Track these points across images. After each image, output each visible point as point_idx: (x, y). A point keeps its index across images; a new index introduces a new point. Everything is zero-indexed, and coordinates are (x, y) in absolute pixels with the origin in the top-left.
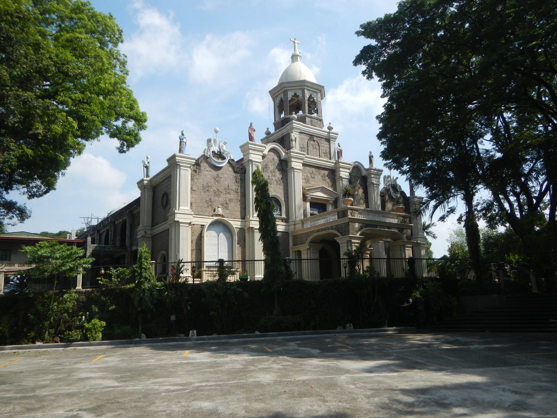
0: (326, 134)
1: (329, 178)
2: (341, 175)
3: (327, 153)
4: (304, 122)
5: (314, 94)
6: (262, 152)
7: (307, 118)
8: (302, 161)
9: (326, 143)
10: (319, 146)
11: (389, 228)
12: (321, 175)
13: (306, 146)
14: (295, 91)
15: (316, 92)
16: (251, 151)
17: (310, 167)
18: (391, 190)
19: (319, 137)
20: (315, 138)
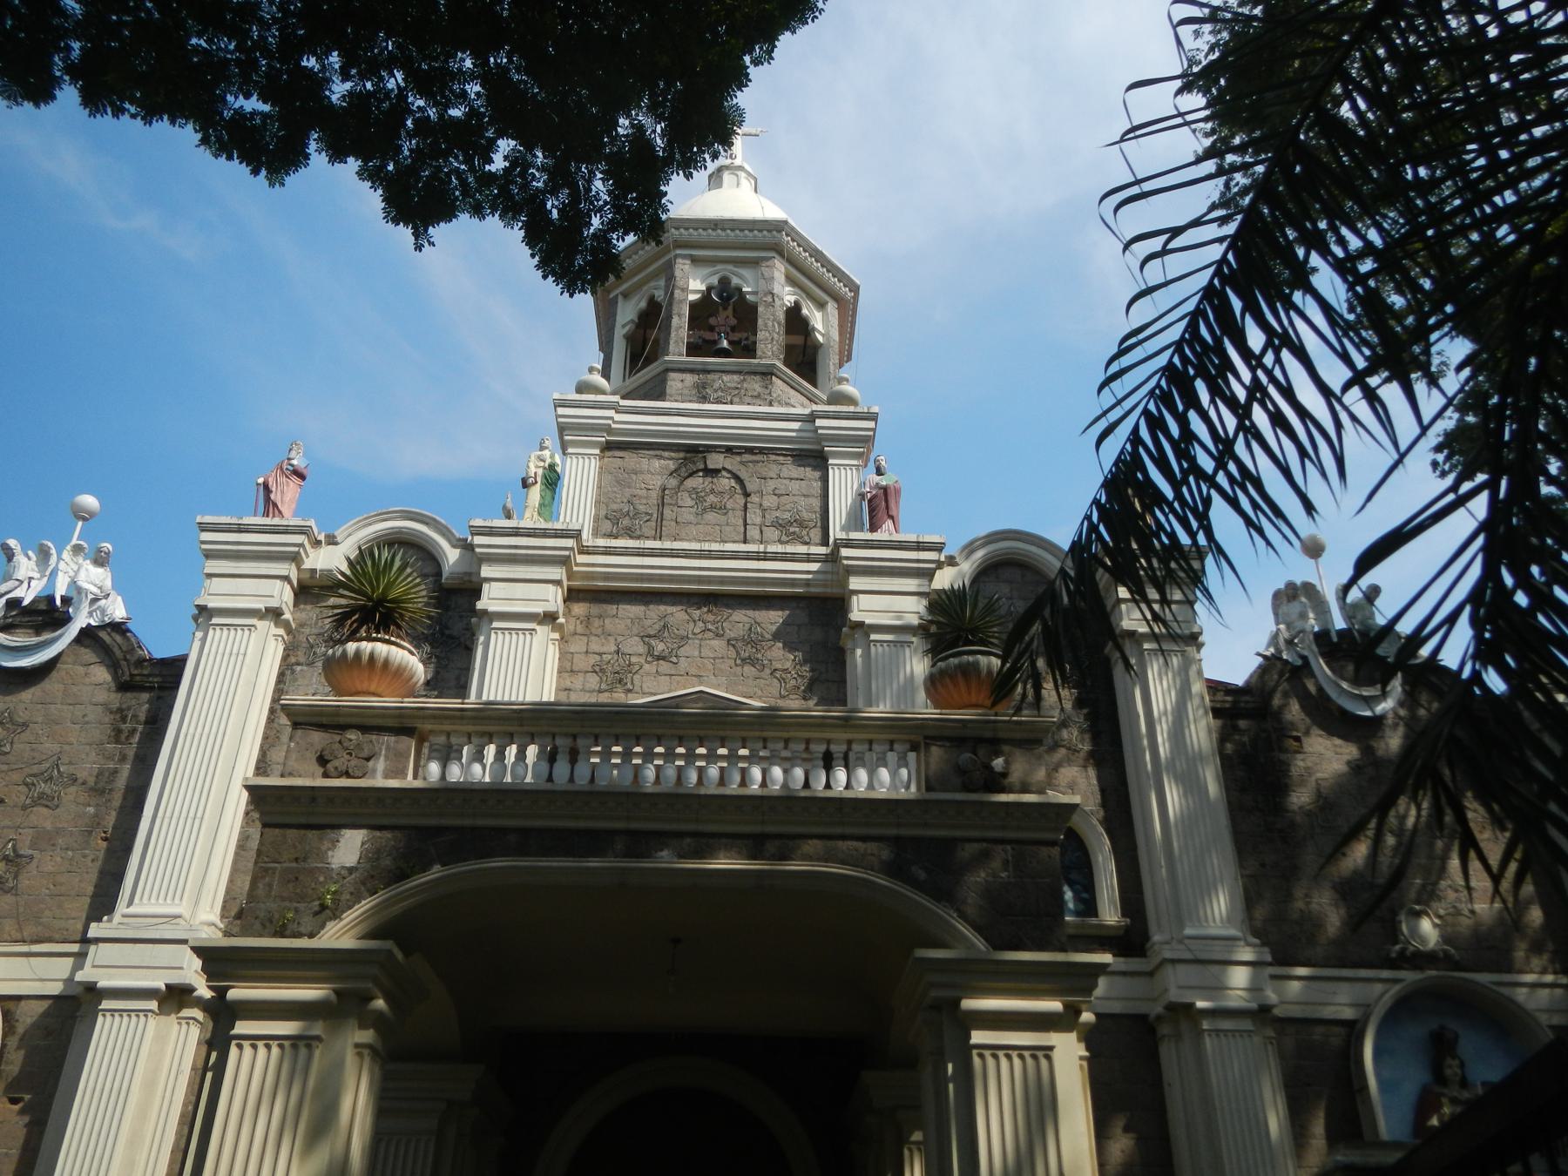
0: (796, 425)
1: (790, 647)
2: (855, 616)
3: (801, 524)
4: (661, 396)
5: (746, 273)
6: (295, 558)
7: (672, 375)
8: (557, 573)
9: (791, 470)
10: (747, 495)
11: (755, 845)
12: (730, 634)
13: (648, 503)
14: (647, 289)
15: (754, 263)
16: (213, 566)
17: (646, 603)
18: (1321, 667)
19: (750, 450)
20: (716, 461)
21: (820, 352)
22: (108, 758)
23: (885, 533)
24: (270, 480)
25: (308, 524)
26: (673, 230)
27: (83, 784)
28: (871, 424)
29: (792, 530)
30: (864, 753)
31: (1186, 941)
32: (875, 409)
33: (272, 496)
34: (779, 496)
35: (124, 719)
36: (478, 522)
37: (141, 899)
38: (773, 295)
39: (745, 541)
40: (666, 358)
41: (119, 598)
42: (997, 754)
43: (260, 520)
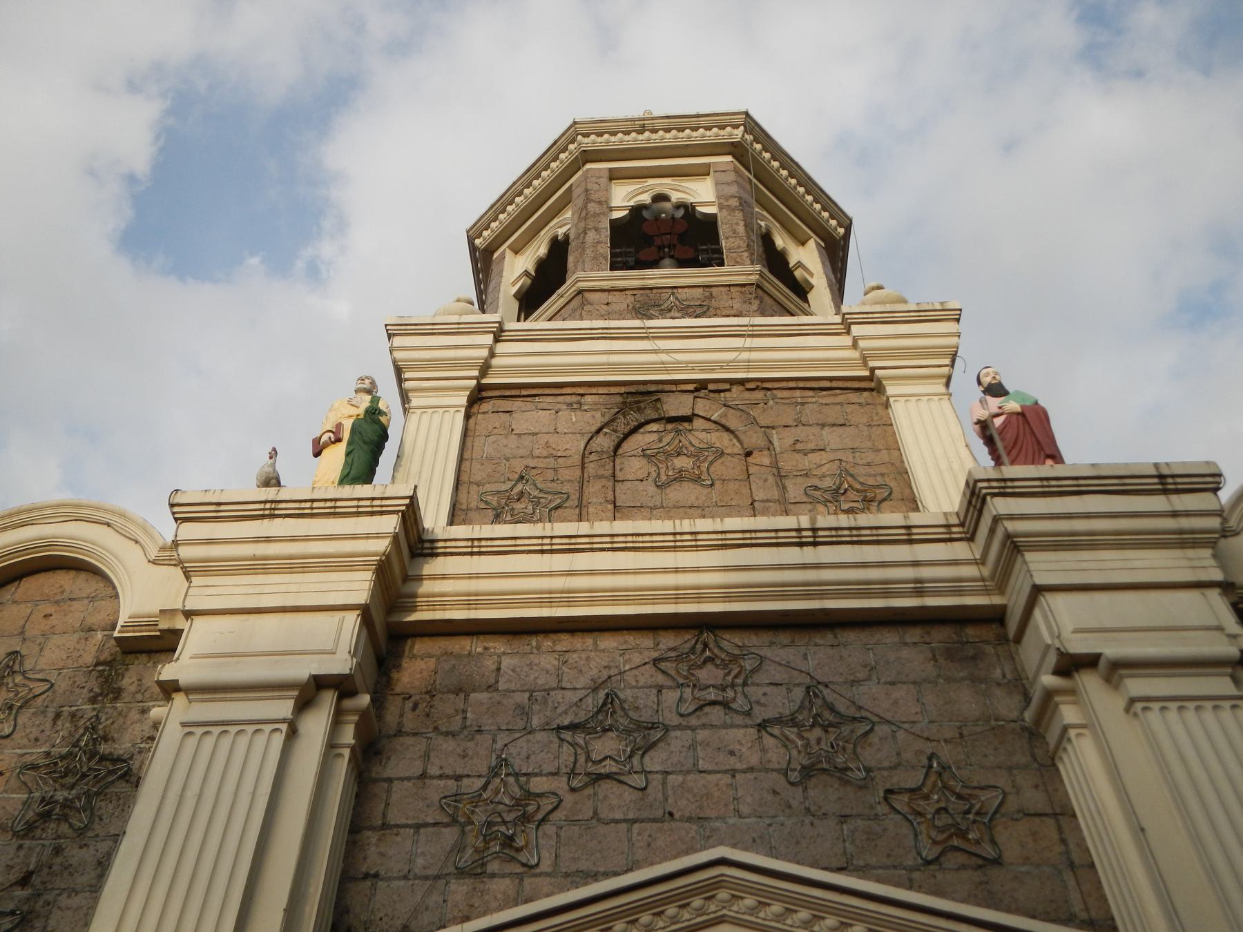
20: (676, 405)
26: (580, 137)
28: (950, 327)
29: (845, 506)
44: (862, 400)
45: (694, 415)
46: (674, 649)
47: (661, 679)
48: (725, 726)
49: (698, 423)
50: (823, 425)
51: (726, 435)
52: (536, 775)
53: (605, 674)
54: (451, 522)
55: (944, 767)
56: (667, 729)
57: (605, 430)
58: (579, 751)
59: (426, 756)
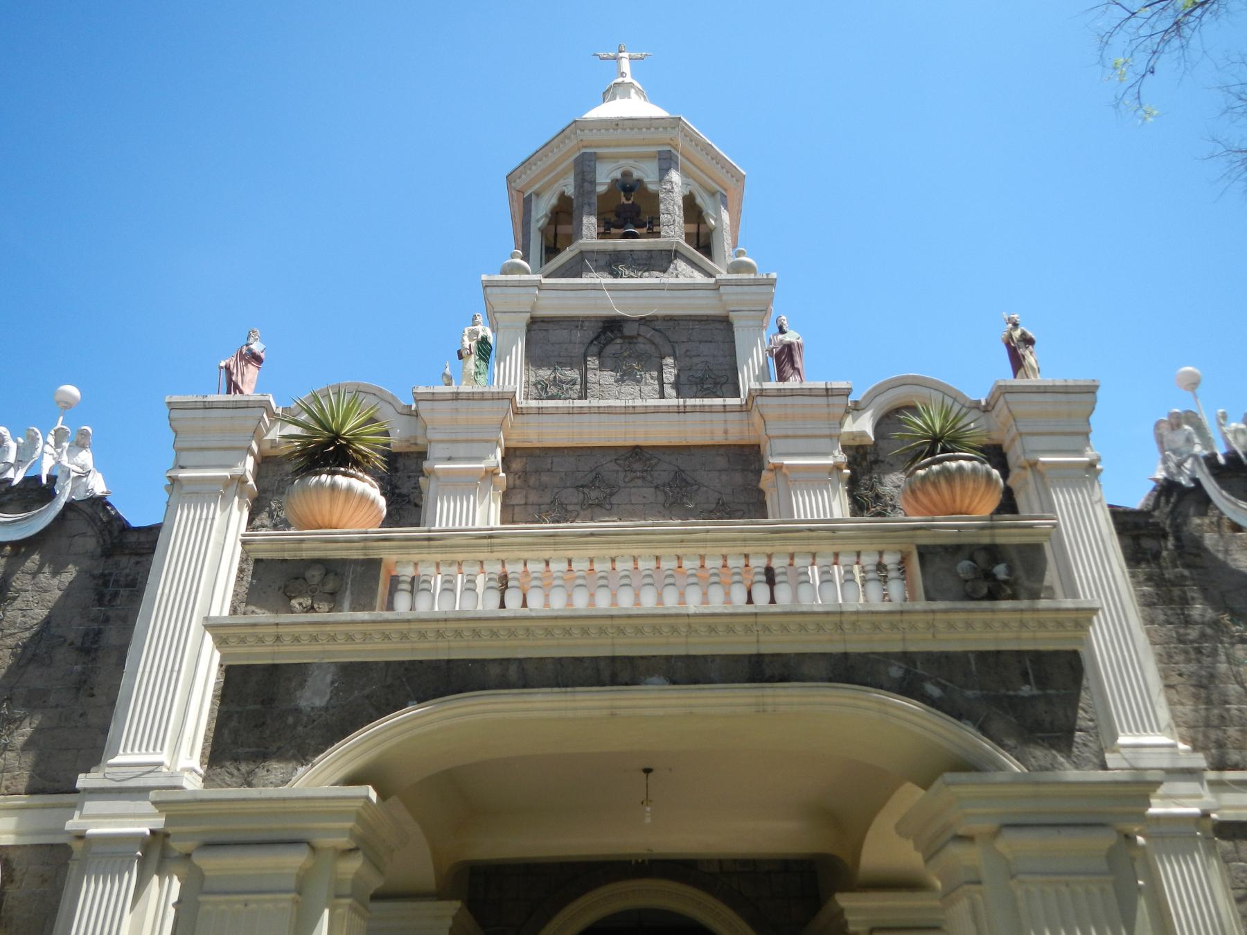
20: (629, 330)
21: (715, 235)
22: (92, 621)
23: (793, 383)
24: (232, 364)
25: (266, 398)
27: (72, 644)
29: (705, 386)
30: (852, 566)
31: (1122, 750)
32: (774, 275)
33: (234, 378)
34: (691, 357)
35: (106, 584)
36: (421, 389)
37: (124, 750)
38: (672, 182)
39: (662, 396)
40: (581, 241)
41: (99, 476)
42: (996, 561)
43: (223, 397)
44: (722, 327)
45: (639, 335)
46: (623, 455)
47: (617, 468)
48: (642, 487)
49: (640, 339)
50: (701, 342)
51: (654, 347)
52: (569, 504)
53: (596, 465)
54: (527, 399)
55: (723, 503)
56: (620, 487)
57: (595, 342)
58: (586, 496)
59: (526, 497)
